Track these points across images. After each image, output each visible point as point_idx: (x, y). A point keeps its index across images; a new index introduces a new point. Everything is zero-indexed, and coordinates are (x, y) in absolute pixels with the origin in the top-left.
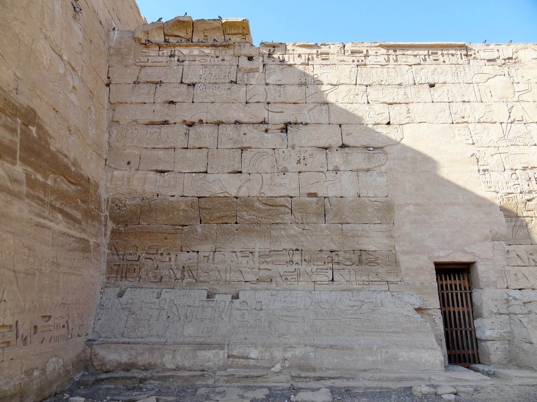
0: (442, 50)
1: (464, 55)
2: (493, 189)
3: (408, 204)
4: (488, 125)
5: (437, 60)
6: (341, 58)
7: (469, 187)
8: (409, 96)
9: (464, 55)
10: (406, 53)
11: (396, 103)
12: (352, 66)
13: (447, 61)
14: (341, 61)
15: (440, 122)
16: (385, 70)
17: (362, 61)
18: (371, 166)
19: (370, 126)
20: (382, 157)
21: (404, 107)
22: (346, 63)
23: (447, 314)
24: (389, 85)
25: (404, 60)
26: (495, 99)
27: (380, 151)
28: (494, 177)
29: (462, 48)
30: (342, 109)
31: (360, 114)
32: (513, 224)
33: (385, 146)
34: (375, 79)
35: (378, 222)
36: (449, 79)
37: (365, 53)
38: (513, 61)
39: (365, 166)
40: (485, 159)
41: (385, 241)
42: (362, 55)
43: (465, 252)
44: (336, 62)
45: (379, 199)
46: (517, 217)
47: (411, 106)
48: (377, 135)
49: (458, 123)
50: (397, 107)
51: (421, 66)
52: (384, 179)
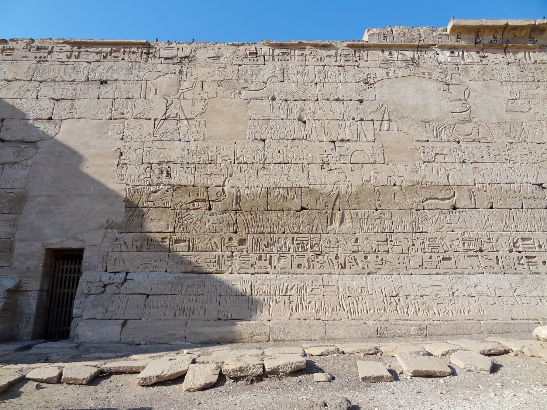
0: (125, 48)
1: (145, 53)
2: (124, 181)
3: (40, 196)
4: (142, 121)
5: (117, 57)
6: (24, 54)
7: (103, 180)
8: (78, 93)
9: (145, 53)
10: (89, 50)
11: (63, 99)
12: (33, 62)
13: (126, 58)
14: (23, 57)
15: (99, 118)
16: (63, 66)
17: (45, 57)
18: (19, 159)
19: (31, 121)
20: (32, 151)
21: (69, 103)
22: (28, 59)
23: (62, 295)
24: (63, 81)
25: (85, 57)
26: (158, 96)
27: (32, 146)
28: (131, 170)
29: (145, 46)
30: (8, 105)
31: (24, 110)
32: (131, 213)
33: (38, 141)
34: (50, 75)
35: (6, 212)
36: (122, 77)
37: (49, 49)
38: (189, 59)
39: (12, 159)
40: (128, 153)
41: (9, 230)
42: (47, 51)
43: (76, 239)
44: (18, 58)
45: (14, 191)
46: (137, 206)
47: (76, 102)
48: (34, 130)
49: (115, 119)
50: (62, 103)
51: (99, 63)
52: (26, 172)
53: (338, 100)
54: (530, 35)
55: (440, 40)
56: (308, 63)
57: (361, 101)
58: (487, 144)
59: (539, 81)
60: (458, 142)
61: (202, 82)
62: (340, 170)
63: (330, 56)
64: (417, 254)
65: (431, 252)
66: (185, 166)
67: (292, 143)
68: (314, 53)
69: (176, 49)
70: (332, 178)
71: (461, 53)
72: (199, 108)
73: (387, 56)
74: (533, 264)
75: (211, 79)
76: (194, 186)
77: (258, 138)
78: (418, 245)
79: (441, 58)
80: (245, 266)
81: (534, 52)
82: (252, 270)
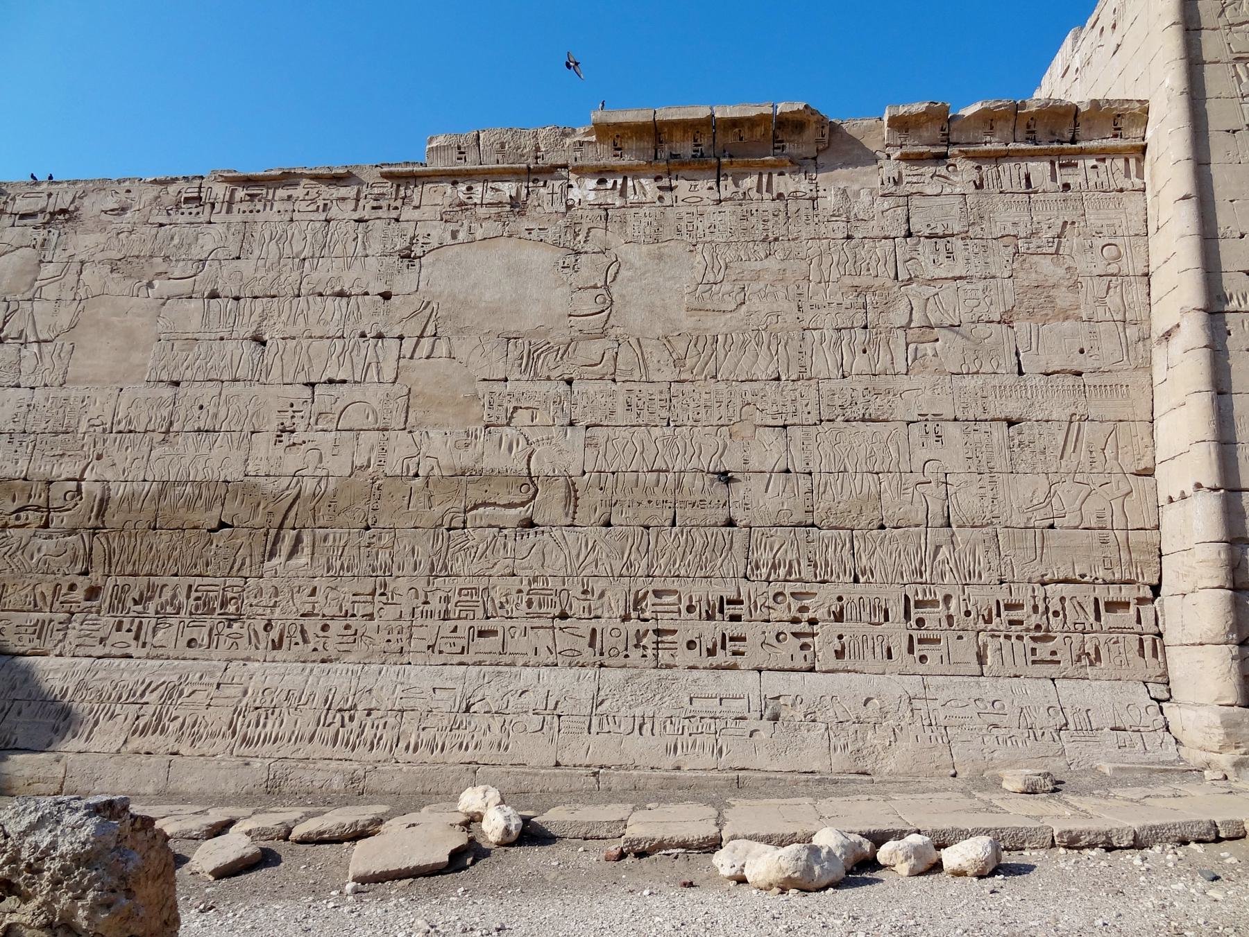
53: (341, 294)
54: (775, 136)
55: (578, 154)
56: (296, 216)
57: (386, 296)
58: (628, 386)
59: (776, 239)
60: (569, 382)
61: (82, 263)
62: (310, 445)
63: (344, 199)
64: (429, 622)
65: (459, 618)
66: (17, 438)
67: (229, 390)
68: (313, 194)
69: (45, 195)
70: (292, 462)
71: (620, 181)
72: (64, 319)
73: (461, 195)
74: (667, 646)
75: (99, 257)
76: (25, 479)
77: (165, 378)
78: (436, 605)
79: (575, 194)
80: (88, 641)
81: (781, 174)
82: (99, 650)
